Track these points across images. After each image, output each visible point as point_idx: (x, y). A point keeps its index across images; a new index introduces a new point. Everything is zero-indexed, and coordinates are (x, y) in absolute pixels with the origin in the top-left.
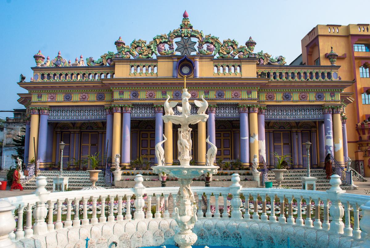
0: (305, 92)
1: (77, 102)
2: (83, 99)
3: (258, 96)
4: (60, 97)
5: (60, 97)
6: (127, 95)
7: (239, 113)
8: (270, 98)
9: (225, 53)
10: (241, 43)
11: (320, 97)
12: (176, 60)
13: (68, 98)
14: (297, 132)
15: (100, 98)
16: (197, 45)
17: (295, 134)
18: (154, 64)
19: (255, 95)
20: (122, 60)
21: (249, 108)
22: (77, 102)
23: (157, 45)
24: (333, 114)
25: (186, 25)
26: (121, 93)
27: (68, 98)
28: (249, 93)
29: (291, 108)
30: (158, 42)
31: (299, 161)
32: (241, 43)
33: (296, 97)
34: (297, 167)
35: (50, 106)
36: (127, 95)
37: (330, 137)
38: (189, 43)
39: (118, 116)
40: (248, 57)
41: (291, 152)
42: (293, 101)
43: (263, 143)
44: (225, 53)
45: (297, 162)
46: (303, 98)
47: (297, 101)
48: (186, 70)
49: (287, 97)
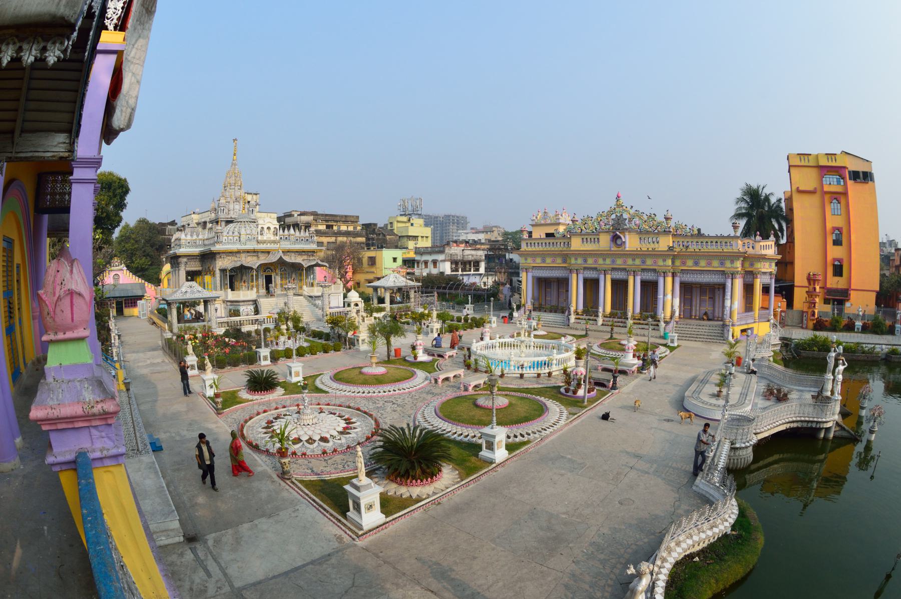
0: (711, 260)
1: (549, 264)
2: (553, 262)
3: (673, 262)
4: (539, 260)
5: (539, 260)
6: (580, 261)
7: (658, 276)
8: (684, 263)
9: (647, 227)
10: (660, 218)
11: (722, 264)
12: (612, 234)
13: (544, 261)
14: (719, 288)
15: (565, 261)
16: (627, 221)
17: (717, 290)
18: (598, 237)
19: (669, 262)
20: (576, 234)
21: (664, 273)
22: (549, 264)
23: (599, 222)
24: (732, 279)
25: (619, 206)
26: (576, 259)
27: (544, 261)
28: (664, 260)
29: (701, 272)
30: (599, 219)
31: (719, 314)
32: (660, 218)
33: (703, 263)
34: (716, 319)
35: (533, 267)
36: (580, 261)
37: (727, 299)
38: (621, 219)
39: (574, 276)
40: (665, 231)
41: (714, 306)
42: (701, 267)
43: (677, 301)
44: (647, 227)
45: (717, 314)
46: (709, 264)
47: (704, 267)
48: (619, 242)
49: (696, 264)
